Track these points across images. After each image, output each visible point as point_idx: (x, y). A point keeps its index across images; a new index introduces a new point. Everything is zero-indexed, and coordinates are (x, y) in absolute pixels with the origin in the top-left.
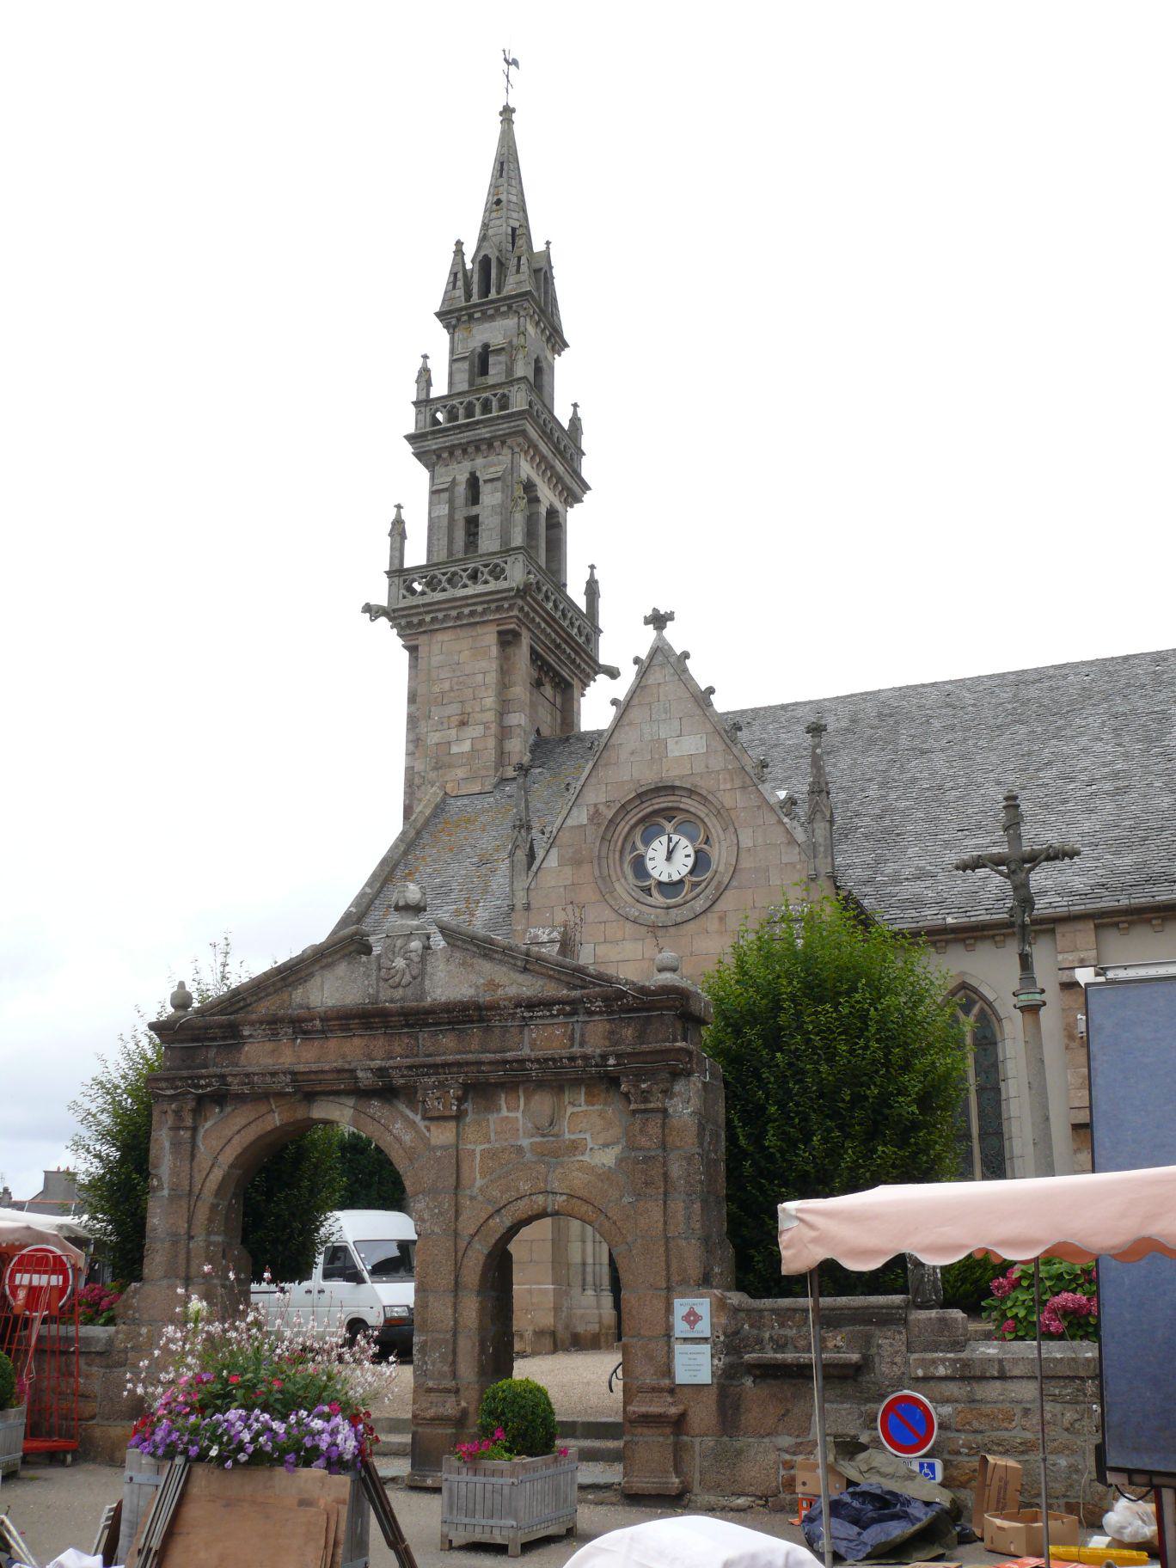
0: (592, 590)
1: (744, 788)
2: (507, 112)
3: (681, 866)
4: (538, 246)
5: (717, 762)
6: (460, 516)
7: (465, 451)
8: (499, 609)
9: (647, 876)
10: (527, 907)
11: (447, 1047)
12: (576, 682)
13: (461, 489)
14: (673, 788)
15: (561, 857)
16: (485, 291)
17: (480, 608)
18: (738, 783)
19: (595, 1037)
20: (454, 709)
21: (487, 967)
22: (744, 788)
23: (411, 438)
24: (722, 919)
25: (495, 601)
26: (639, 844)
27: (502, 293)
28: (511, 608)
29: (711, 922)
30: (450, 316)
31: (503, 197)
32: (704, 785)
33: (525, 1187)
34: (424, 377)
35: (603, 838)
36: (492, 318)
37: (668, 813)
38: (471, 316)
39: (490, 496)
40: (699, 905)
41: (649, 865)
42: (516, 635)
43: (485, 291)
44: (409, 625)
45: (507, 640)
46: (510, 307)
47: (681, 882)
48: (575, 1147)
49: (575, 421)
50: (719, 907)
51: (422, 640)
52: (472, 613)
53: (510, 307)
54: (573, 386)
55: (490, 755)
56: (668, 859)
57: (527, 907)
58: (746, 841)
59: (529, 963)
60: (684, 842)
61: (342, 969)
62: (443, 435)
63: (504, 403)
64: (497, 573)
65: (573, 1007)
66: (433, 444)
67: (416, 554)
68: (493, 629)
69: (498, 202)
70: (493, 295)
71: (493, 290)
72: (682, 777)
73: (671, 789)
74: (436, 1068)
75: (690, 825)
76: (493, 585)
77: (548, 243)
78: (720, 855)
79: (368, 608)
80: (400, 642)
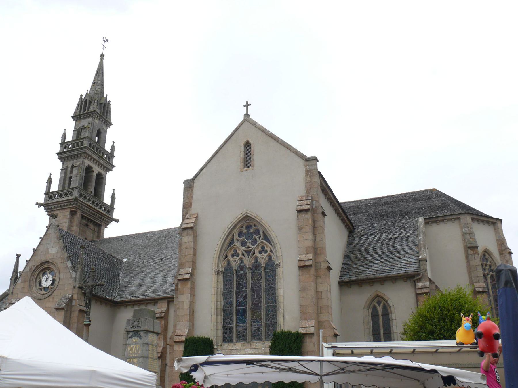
0: (113, 197)
2: (102, 56)
3: (50, 282)
6: (68, 177)
7: (71, 158)
8: (70, 204)
10: (12, 294)
12: (102, 224)
13: (69, 169)
14: (49, 262)
15: (22, 280)
16: (84, 110)
17: (66, 204)
18: (62, 261)
23: (58, 154)
24: (53, 298)
25: (69, 202)
26: (41, 277)
27: (94, 110)
29: (51, 299)
30: (75, 117)
34: (64, 136)
35: (31, 275)
36: (85, 118)
37: (49, 269)
38: (80, 117)
39: (75, 171)
43: (84, 110)
44: (48, 209)
45: (73, 213)
47: (48, 288)
49: (113, 148)
50: (54, 294)
52: (64, 206)
54: (112, 137)
57: (12, 294)
58: (62, 277)
60: (51, 276)
62: (67, 153)
64: (71, 193)
66: (63, 156)
67: (55, 187)
68: (69, 210)
70: (86, 112)
75: (51, 271)
76: (70, 197)
79: (37, 204)
80: (46, 213)
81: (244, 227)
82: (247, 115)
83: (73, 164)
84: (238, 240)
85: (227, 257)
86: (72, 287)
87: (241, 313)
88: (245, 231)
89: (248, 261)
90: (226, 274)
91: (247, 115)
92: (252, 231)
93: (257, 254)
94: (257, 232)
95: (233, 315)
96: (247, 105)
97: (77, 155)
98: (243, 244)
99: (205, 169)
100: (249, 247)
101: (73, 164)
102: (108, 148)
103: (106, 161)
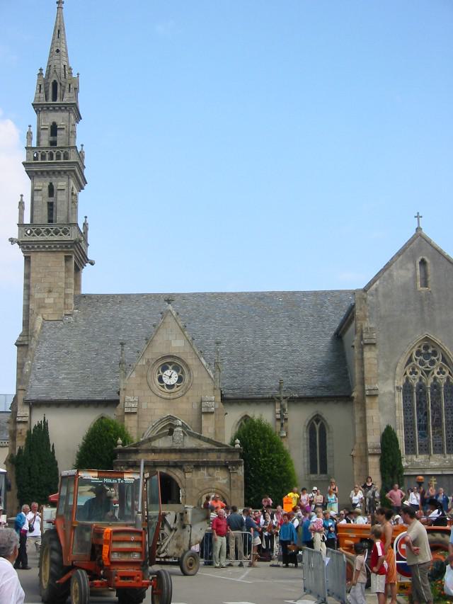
1: (195, 358)
3: (174, 380)
5: (188, 349)
9: (163, 382)
11: (190, 457)
19: (223, 457)
20: (46, 285)
21: (198, 441)
22: (195, 358)
23: (24, 164)
24: (188, 398)
28: (71, 247)
29: (184, 399)
32: (183, 357)
33: (207, 486)
36: (57, 111)
38: (48, 108)
40: (180, 393)
42: (71, 257)
43: (55, 98)
45: (67, 259)
46: (66, 108)
48: (217, 479)
50: (187, 394)
51: (32, 255)
53: (66, 108)
56: (171, 377)
59: (208, 441)
60: (175, 373)
61: (163, 438)
63: (66, 157)
65: (219, 451)
71: (58, 98)
73: (173, 357)
74: (188, 462)
76: (65, 238)
83: (51, 184)
84: (416, 360)
85: (405, 374)
86: (212, 387)
87: (423, 428)
88: (423, 351)
89: (429, 382)
92: (430, 351)
93: (436, 374)
95: (414, 430)
97: (59, 172)
98: (422, 363)
101: (51, 184)
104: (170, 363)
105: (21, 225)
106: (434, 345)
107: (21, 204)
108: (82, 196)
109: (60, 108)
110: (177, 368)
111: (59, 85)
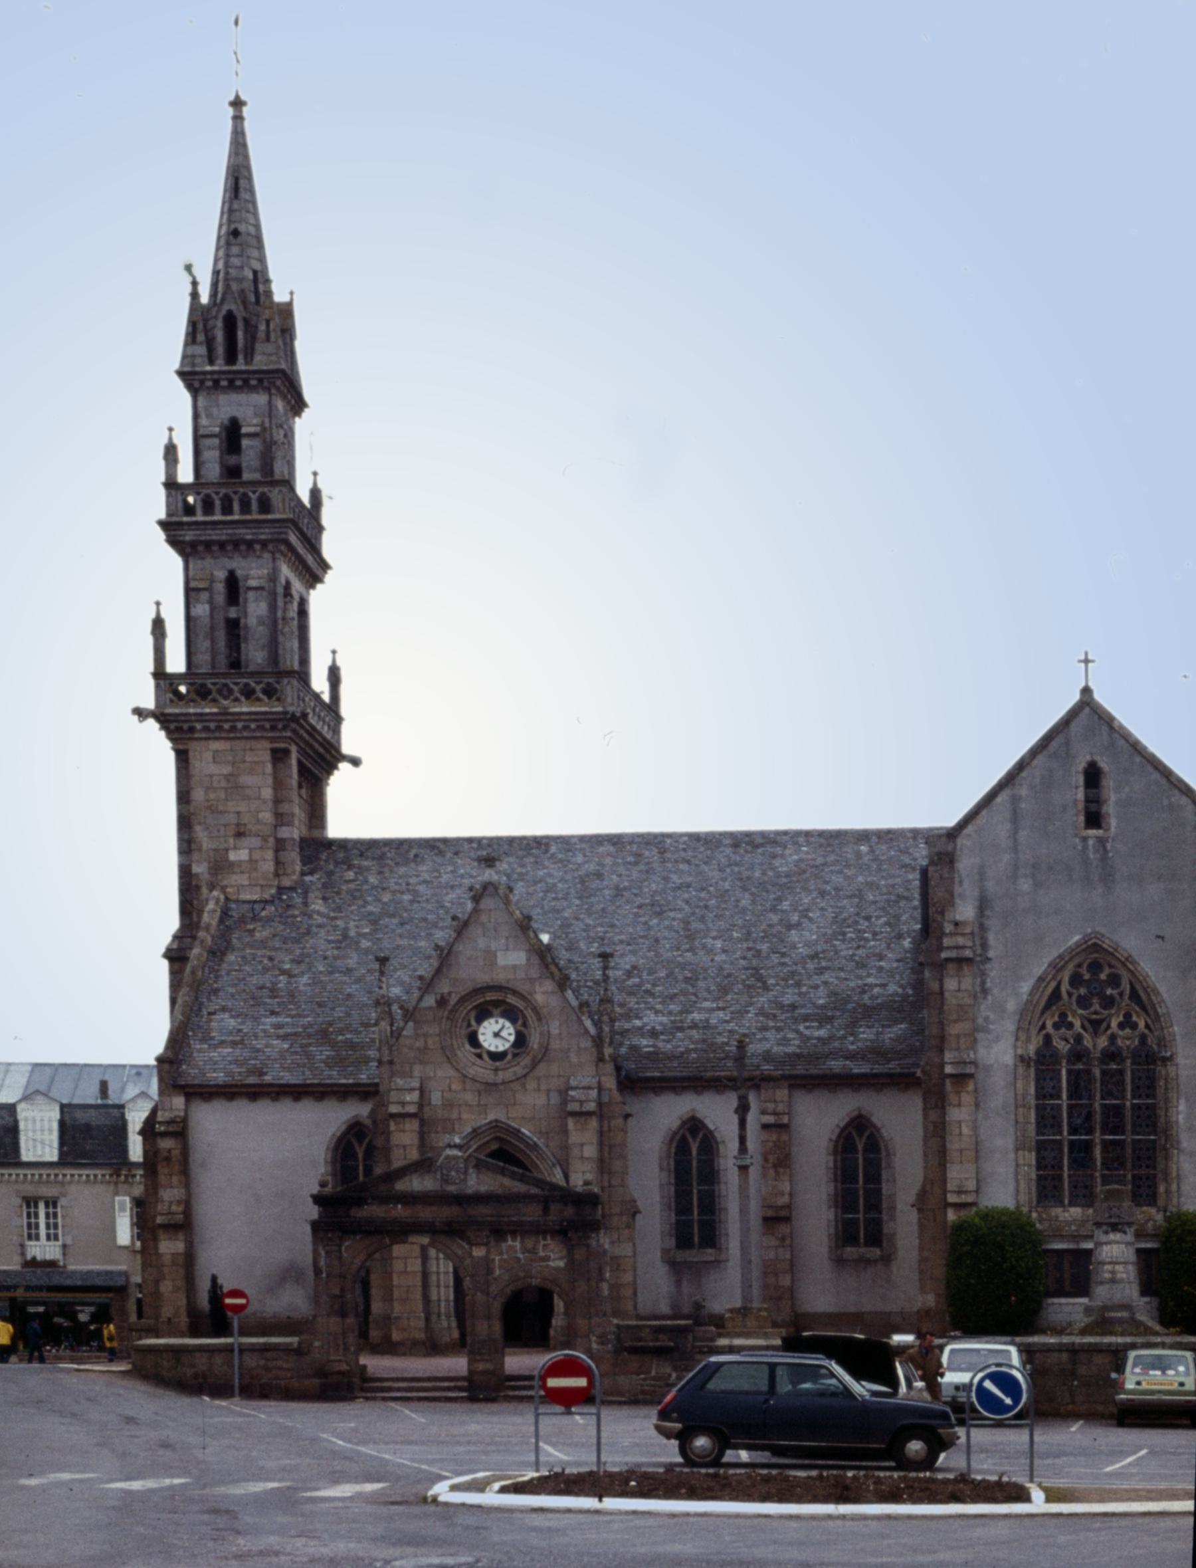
0: (334, 676)
4: (280, 296)
8: (273, 728)
13: (220, 587)
17: (253, 726)
23: (163, 524)
26: (473, 1023)
28: (285, 728)
31: (242, 228)
32: (523, 988)
36: (239, 389)
38: (216, 382)
40: (519, 1070)
41: (481, 1038)
42: (287, 752)
43: (231, 358)
45: (279, 756)
49: (315, 494)
53: (260, 381)
55: (268, 866)
56: (495, 1034)
60: (508, 1024)
69: (235, 233)
70: (240, 365)
71: (241, 357)
72: (508, 981)
77: (292, 293)
78: (535, 1041)
81: (1085, 966)
82: (1086, 691)
85: (1043, 1027)
88: (1087, 977)
90: (1043, 1064)
91: (1086, 691)
94: (1114, 980)
96: (1086, 661)
98: (1083, 1002)
99: (984, 813)
100: (1096, 1013)
102: (303, 493)
103: (296, 538)
104: (496, 1003)
105: (160, 674)
106: (1113, 962)
107: (158, 626)
108: (319, 600)
109: (246, 381)
110: (511, 1014)
111: (240, 325)
